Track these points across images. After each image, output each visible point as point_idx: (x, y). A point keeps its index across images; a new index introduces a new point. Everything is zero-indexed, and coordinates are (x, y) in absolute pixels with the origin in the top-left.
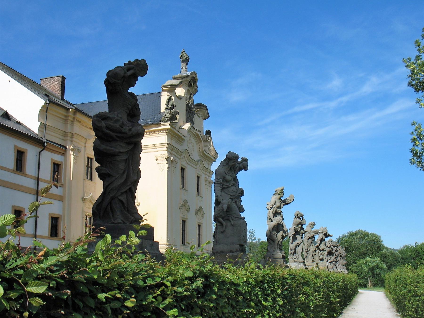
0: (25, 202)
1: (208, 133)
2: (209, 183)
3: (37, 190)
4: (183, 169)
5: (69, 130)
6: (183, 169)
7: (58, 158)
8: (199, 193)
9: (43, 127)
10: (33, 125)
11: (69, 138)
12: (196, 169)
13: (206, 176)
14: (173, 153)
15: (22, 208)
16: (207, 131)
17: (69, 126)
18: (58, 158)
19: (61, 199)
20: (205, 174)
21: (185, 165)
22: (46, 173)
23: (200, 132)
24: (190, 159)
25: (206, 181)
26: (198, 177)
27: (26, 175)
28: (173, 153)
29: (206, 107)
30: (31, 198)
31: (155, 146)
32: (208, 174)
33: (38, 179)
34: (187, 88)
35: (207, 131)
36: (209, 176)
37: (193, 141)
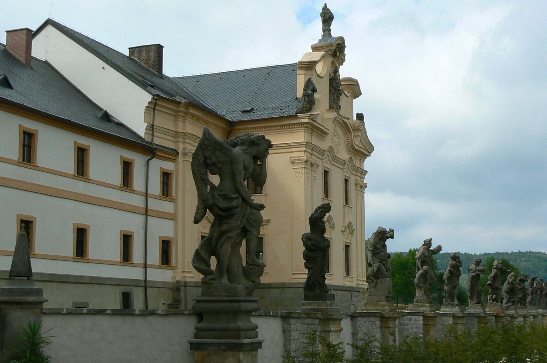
0: (133, 224)
1: (360, 117)
2: (361, 187)
3: (146, 209)
4: (326, 173)
6: (326, 173)
7: (169, 166)
8: (347, 203)
9: (152, 128)
10: (139, 126)
11: (180, 139)
12: (343, 169)
13: (358, 178)
14: (314, 153)
16: (358, 115)
17: (180, 124)
18: (169, 166)
19: (172, 217)
20: (356, 175)
21: (328, 165)
23: (348, 119)
24: (336, 159)
25: (356, 185)
26: (346, 181)
27: (133, 191)
28: (314, 153)
29: (356, 81)
30: (140, 219)
31: (290, 146)
32: (359, 175)
33: (146, 195)
34: (330, 59)
35: (358, 115)
36: (361, 178)
37: (339, 132)
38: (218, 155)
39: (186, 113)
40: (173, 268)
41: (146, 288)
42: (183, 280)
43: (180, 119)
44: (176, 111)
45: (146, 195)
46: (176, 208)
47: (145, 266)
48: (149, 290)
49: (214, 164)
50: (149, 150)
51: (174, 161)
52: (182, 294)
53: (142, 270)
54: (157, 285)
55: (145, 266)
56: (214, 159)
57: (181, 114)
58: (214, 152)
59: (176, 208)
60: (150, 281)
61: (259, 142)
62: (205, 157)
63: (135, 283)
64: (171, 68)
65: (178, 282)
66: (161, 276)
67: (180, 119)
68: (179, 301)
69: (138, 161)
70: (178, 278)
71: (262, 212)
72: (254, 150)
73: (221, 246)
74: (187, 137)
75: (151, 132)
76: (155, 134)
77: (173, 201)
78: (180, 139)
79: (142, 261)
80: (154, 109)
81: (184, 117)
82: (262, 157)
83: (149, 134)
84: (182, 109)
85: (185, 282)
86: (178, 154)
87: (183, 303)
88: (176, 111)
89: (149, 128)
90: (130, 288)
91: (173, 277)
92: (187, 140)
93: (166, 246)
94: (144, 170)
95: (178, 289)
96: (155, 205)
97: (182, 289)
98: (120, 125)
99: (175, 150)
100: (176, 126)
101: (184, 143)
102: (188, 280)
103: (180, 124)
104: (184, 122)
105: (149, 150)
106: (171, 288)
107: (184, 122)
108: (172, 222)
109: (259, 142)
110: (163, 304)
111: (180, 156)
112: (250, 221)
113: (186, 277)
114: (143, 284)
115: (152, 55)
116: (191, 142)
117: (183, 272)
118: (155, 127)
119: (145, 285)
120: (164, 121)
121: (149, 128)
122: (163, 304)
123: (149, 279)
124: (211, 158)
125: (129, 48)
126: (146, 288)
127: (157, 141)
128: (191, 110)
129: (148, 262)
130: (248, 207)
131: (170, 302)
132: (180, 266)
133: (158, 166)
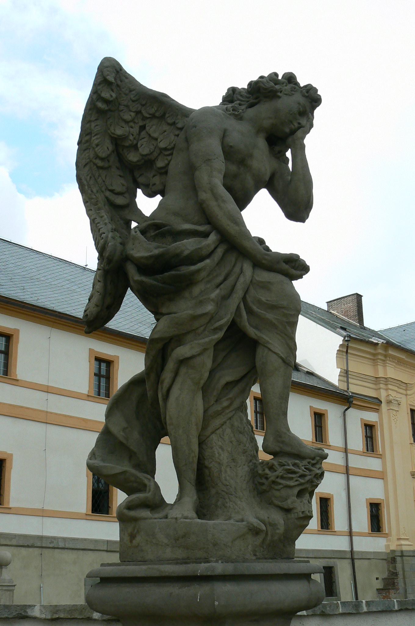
3: (347, 467)
5: (381, 375)
7: (371, 417)
9: (346, 374)
15: (330, 494)
17: (380, 368)
18: (371, 417)
19: (381, 476)
22: (357, 441)
30: (341, 478)
33: (346, 451)
38: (155, 135)
39: (386, 356)
40: (386, 536)
41: (353, 560)
42: (399, 548)
43: (380, 363)
44: (374, 355)
45: (346, 451)
46: (384, 464)
47: (351, 534)
48: (357, 563)
49: (148, 163)
50: (344, 399)
51: (377, 410)
52: (399, 566)
53: (347, 539)
54: (366, 557)
55: (351, 534)
56: (145, 148)
57: (380, 357)
58: (143, 128)
59: (384, 464)
60: (359, 552)
61: (277, 87)
62: (117, 142)
63: (339, 555)
64: (376, 320)
65: (393, 551)
66: (368, 544)
67: (380, 363)
68: (396, 574)
69: (333, 412)
70: (393, 548)
71: (297, 284)
72: (264, 110)
73: (167, 396)
74: (389, 383)
75: (345, 379)
76: (350, 380)
77: (380, 456)
78: (382, 386)
79: (346, 529)
80: (347, 352)
81: (384, 361)
82: (293, 132)
83: (344, 381)
84: (380, 351)
85: (402, 552)
86: (381, 402)
87: (401, 576)
88: (374, 355)
89: (342, 374)
90: (332, 560)
91: (387, 546)
92: (390, 387)
93: (375, 511)
94: (340, 421)
95: (393, 560)
96: (355, 462)
97: (398, 559)
98: (311, 374)
99: (377, 398)
100: (377, 371)
101: (387, 390)
102: (404, 548)
103: (380, 368)
104: (385, 366)
105: (344, 399)
106: (385, 559)
107: (385, 366)
108: (381, 481)
109: (277, 87)
110: (377, 579)
111: (384, 405)
112: (255, 308)
113: (401, 545)
114: (349, 556)
115: (352, 305)
116: (396, 389)
117: (399, 539)
118: (349, 373)
119: (352, 557)
120: (360, 366)
121: (342, 374)
122: (377, 579)
123: (355, 549)
124: (135, 147)
125: (327, 303)
126: (353, 560)
127: (353, 389)
128: (391, 352)
129: (354, 529)
130: (248, 268)
131: (386, 575)
132: (394, 532)
133: (357, 417)
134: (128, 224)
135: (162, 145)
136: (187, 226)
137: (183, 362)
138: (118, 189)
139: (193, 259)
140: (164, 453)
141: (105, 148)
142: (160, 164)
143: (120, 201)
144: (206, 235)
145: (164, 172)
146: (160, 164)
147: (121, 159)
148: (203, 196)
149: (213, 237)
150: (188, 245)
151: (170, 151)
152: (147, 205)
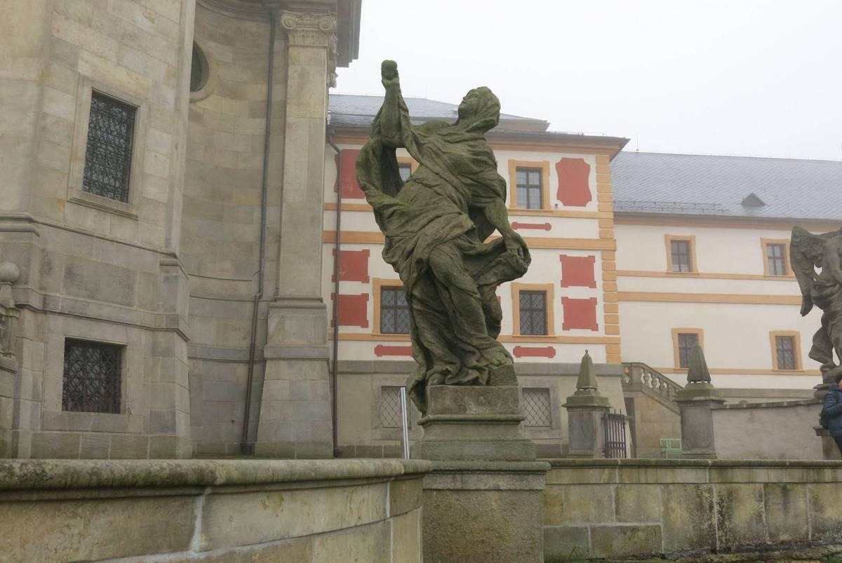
58: (811, 247)
62: (803, 253)
73: (830, 334)
134: (812, 279)
135: (819, 252)
136: (828, 284)
137: (834, 325)
138: (806, 268)
139: (832, 294)
140: (834, 350)
141: (799, 257)
142: (819, 258)
143: (807, 272)
144: (834, 286)
145: (821, 260)
146: (819, 258)
147: (806, 257)
148: (833, 273)
149: (838, 286)
150: (828, 291)
151: (822, 255)
152: (818, 271)
